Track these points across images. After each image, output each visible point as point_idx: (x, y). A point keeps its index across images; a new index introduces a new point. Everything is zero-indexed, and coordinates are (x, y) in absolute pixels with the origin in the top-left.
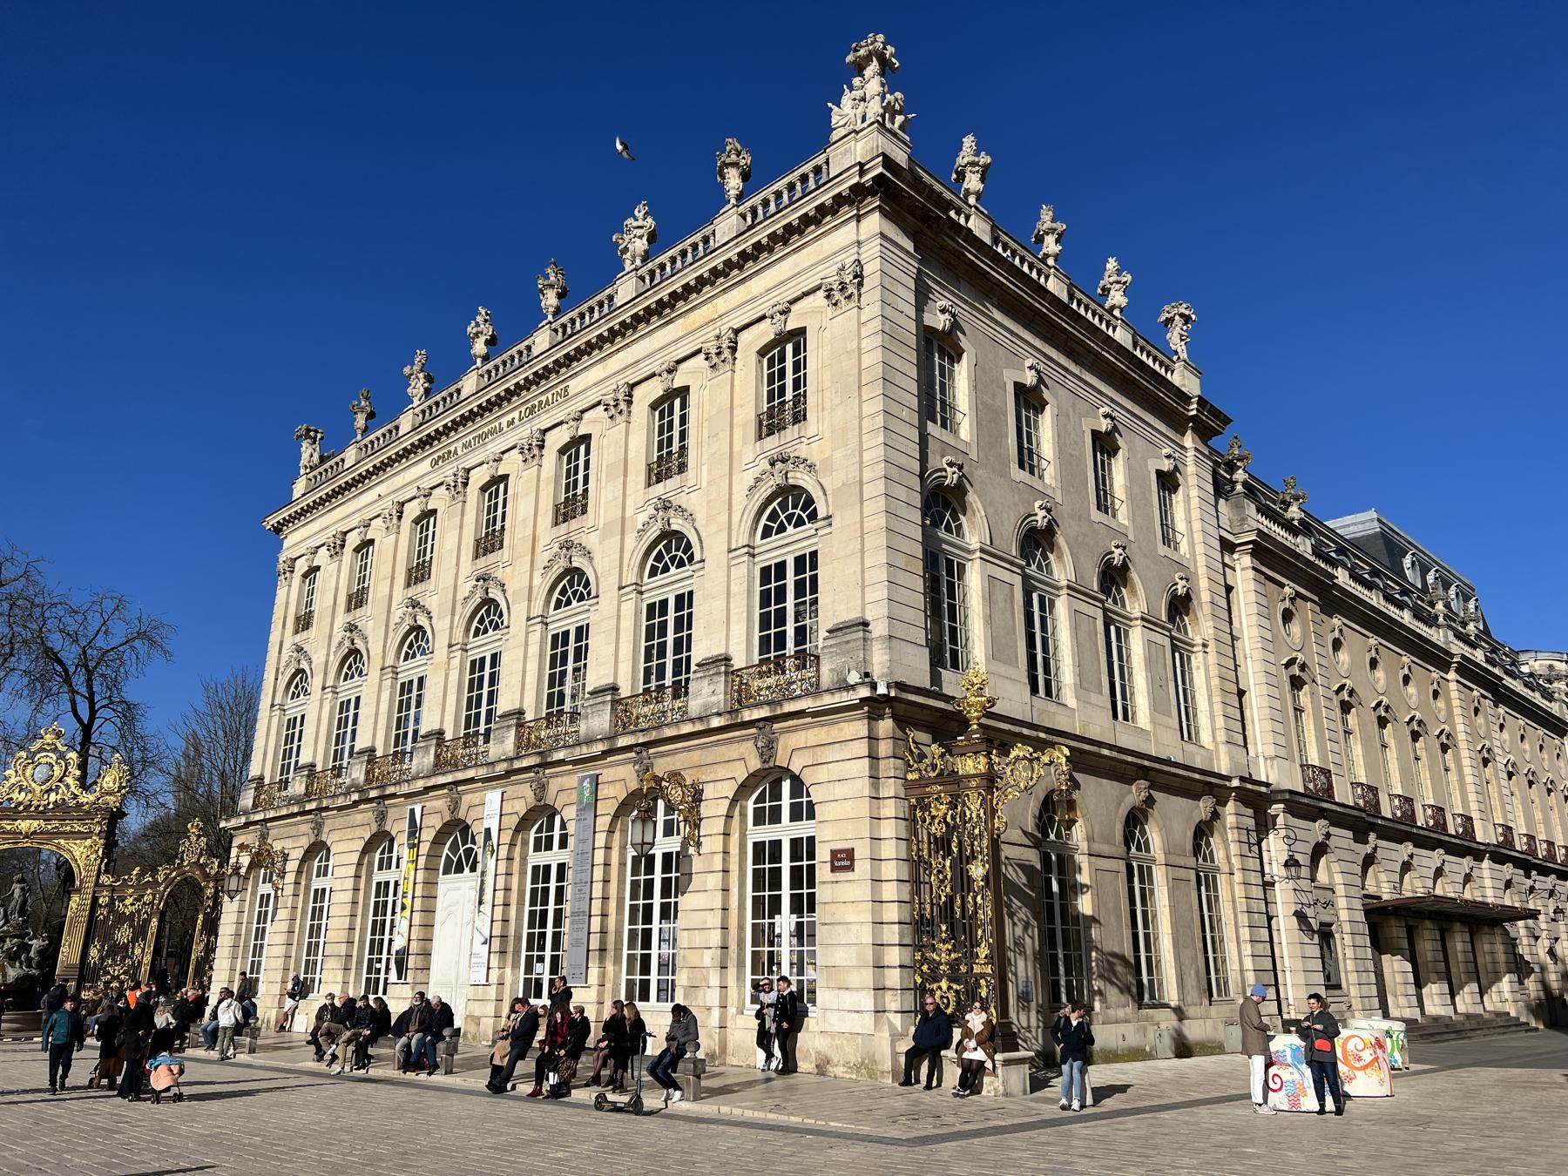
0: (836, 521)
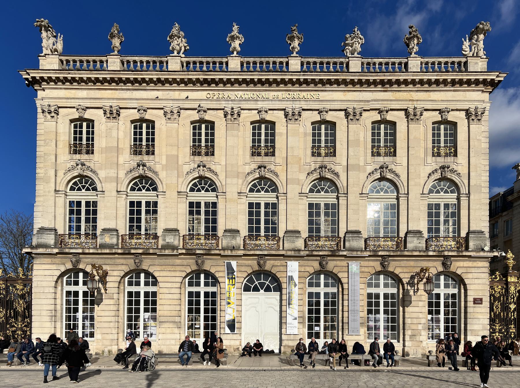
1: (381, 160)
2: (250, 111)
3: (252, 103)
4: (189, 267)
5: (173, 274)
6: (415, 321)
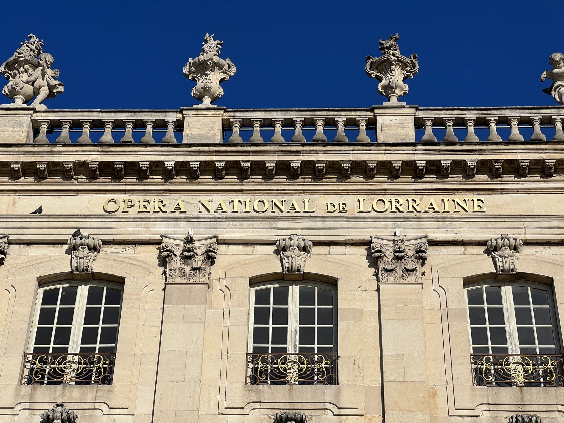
2: (249, 249)
3: (257, 225)
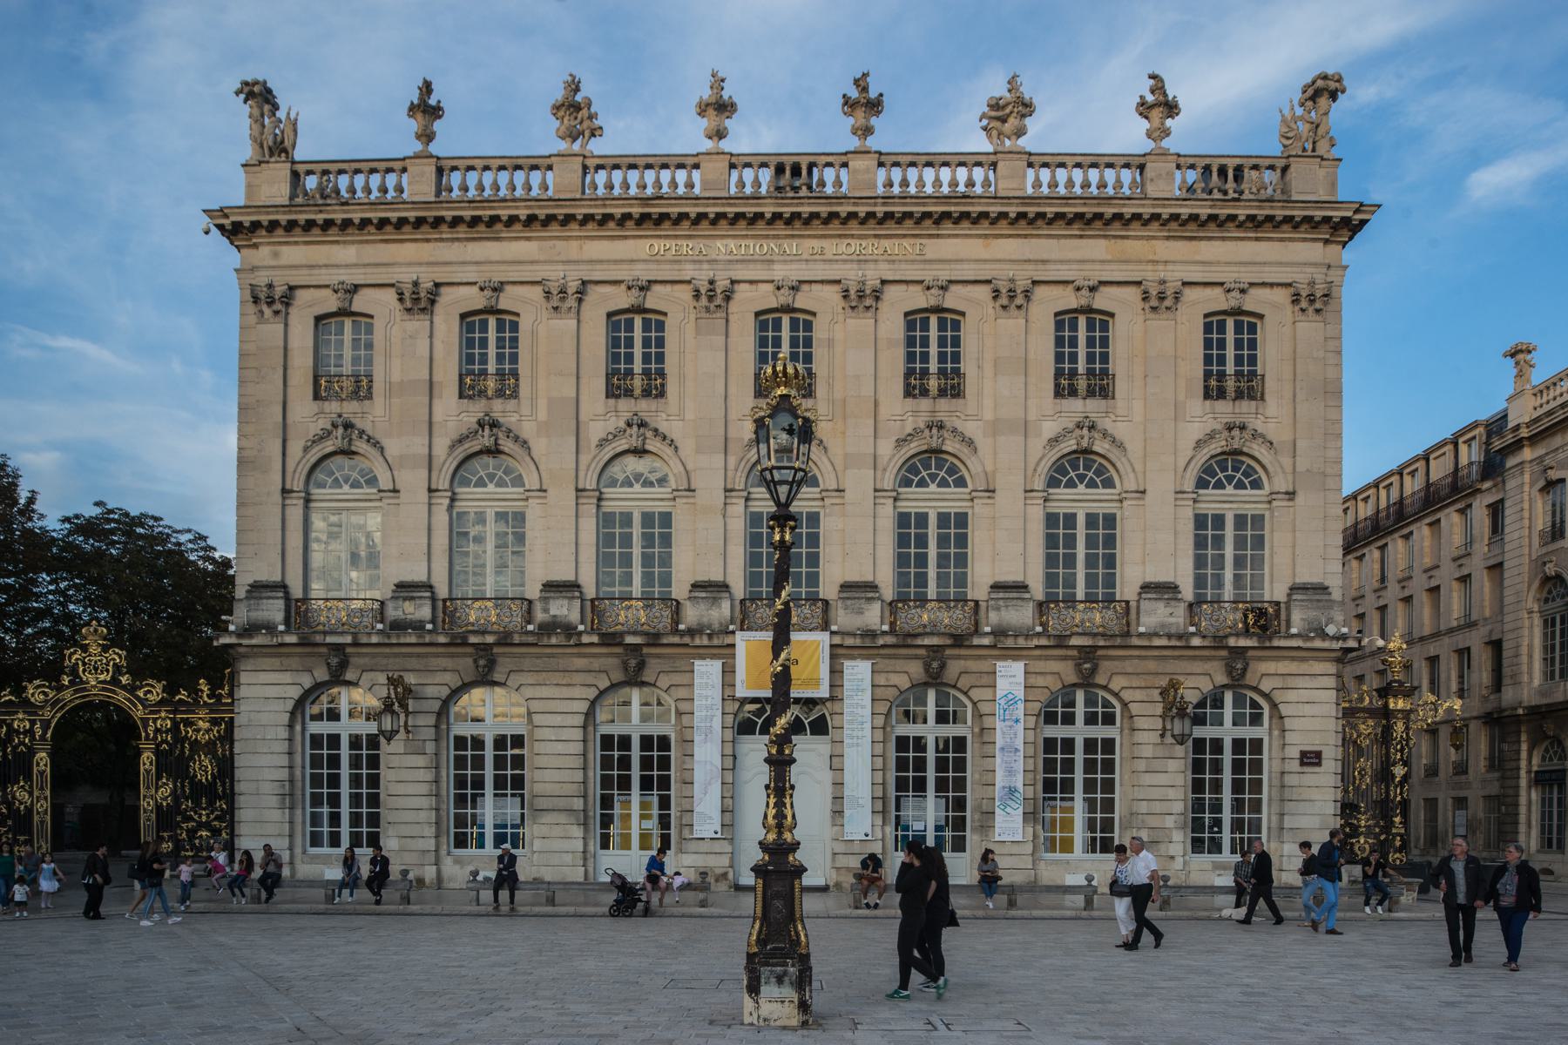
0: (1300, 499)
1: (1077, 407)
2: (754, 287)
4: (604, 675)
5: (566, 692)
6: (1158, 807)
